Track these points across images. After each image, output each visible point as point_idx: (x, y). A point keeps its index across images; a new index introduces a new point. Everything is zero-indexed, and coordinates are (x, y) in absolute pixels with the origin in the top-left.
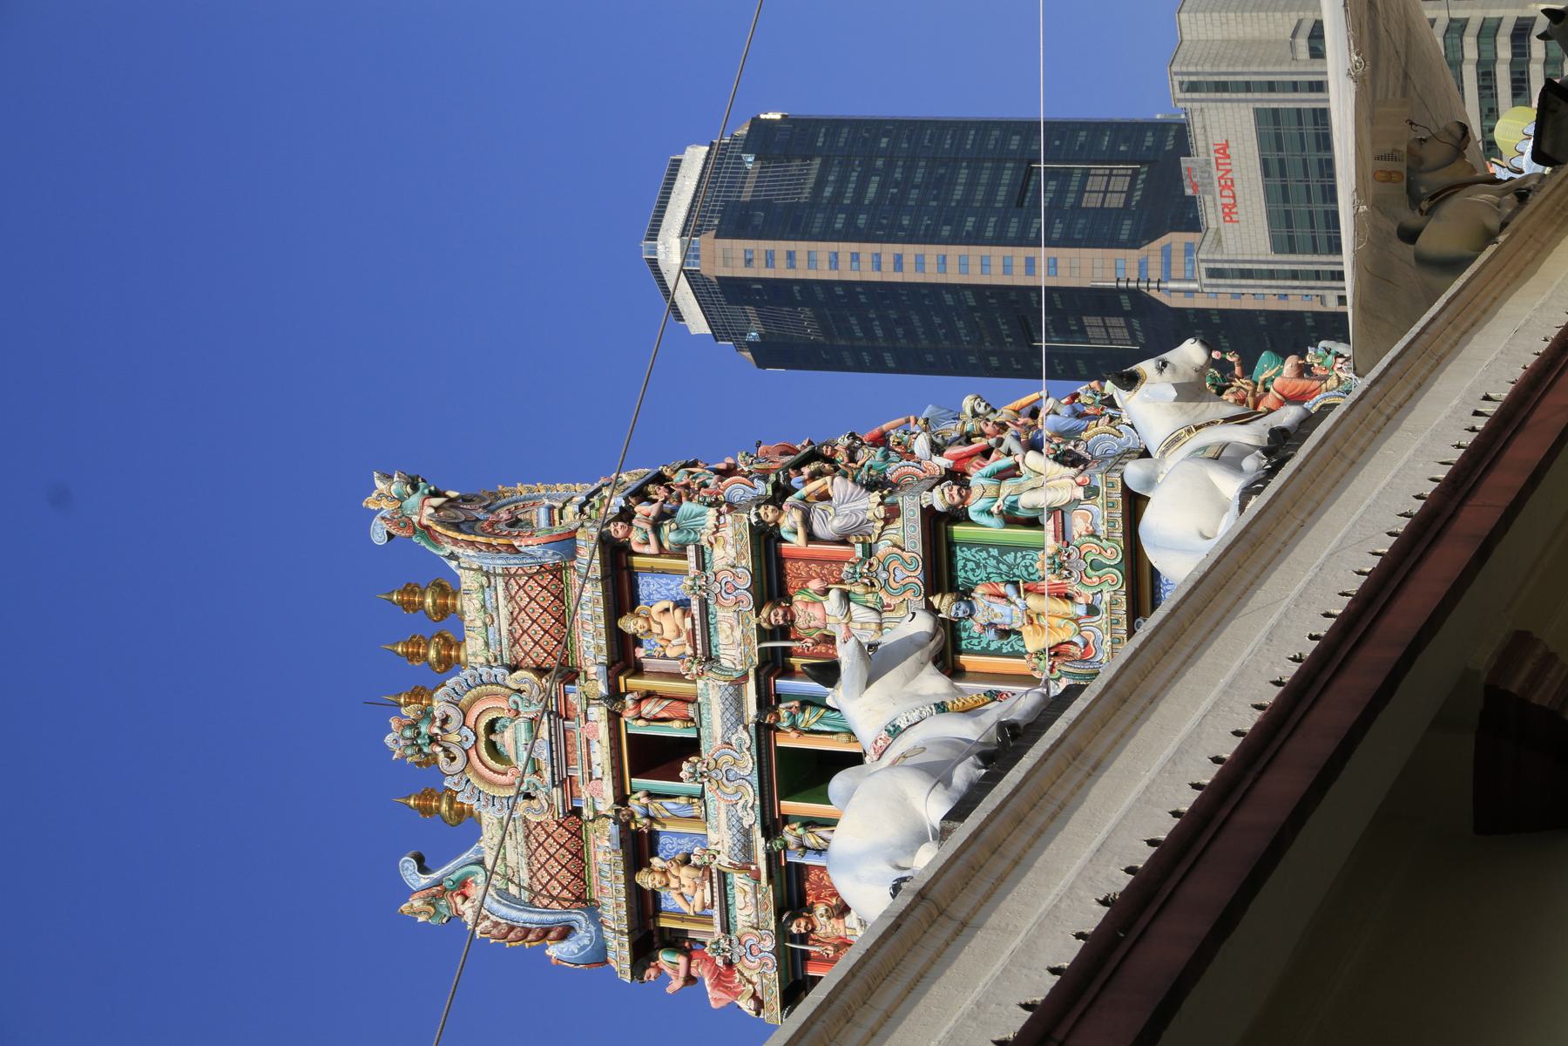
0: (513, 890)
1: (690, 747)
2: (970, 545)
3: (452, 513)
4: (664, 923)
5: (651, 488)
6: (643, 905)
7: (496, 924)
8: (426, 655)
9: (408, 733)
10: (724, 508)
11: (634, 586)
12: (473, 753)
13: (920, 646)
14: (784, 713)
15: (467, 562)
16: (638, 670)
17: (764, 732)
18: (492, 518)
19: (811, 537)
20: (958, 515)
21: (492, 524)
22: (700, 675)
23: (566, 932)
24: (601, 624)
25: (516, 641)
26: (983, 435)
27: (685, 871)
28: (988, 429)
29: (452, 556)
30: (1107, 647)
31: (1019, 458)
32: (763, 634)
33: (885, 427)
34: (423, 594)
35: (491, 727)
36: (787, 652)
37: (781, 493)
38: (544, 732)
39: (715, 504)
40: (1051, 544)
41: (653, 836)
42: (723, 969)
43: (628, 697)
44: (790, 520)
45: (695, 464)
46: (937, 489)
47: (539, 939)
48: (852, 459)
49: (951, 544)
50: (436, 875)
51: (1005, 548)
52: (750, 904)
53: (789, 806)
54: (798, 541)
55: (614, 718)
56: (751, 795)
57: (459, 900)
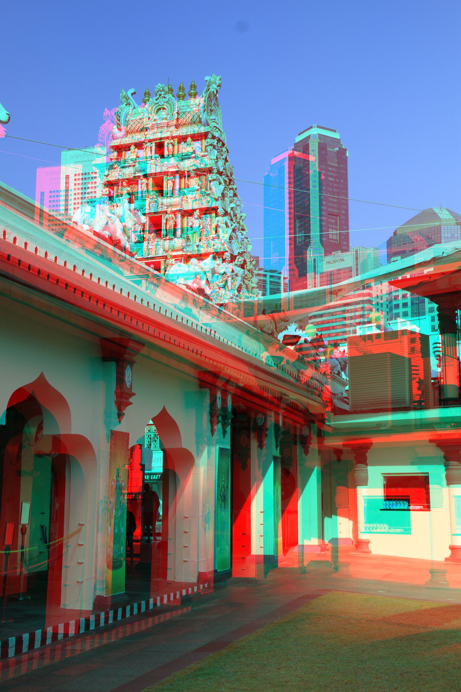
0: (128, 116)
1: (162, 156)
2: (211, 217)
3: (213, 96)
4: (123, 153)
5: (221, 143)
6: (127, 148)
7: (120, 113)
8: (180, 91)
9: (161, 89)
10: (216, 161)
11: (198, 140)
12: (158, 105)
13: (139, 221)
14: (171, 178)
15: (200, 101)
16: (179, 143)
17: (166, 173)
18: (212, 105)
19: (210, 181)
20: (217, 215)
21: (211, 105)
22: (178, 157)
23: (120, 130)
24: (189, 133)
25: (184, 113)
26: (236, 219)
27: (135, 157)
28: (238, 220)
29: (203, 96)
30: (190, 250)
31: (230, 227)
32: (188, 172)
33: (238, 196)
34: (194, 90)
35: (164, 109)
36: (185, 177)
37: (220, 173)
38: (165, 121)
39: (217, 158)
41: (143, 149)
42: (114, 167)
43: (172, 141)
44: (214, 176)
45: (228, 152)
46: (222, 209)
47: (118, 123)
48: (230, 189)
49: (211, 213)
50: (131, 97)
51: (210, 225)
52: (129, 173)
53: (151, 180)
54: (210, 179)
55: (168, 138)
56: (153, 171)
57: (126, 103)
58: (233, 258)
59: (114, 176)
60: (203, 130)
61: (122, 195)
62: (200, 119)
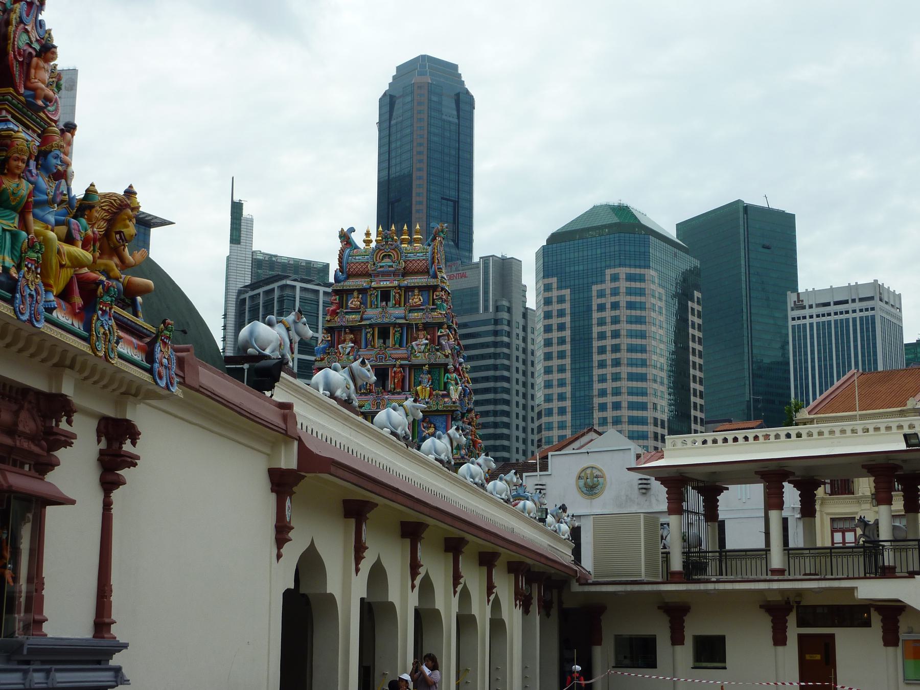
20: (447, 371)
32: (416, 324)
40: (441, 393)
55: (395, 287)
56: (379, 321)
58: (463, 415)
59: (338, 321)
60: (432, 282)
61: (344, 341)
62: (428, 270)
